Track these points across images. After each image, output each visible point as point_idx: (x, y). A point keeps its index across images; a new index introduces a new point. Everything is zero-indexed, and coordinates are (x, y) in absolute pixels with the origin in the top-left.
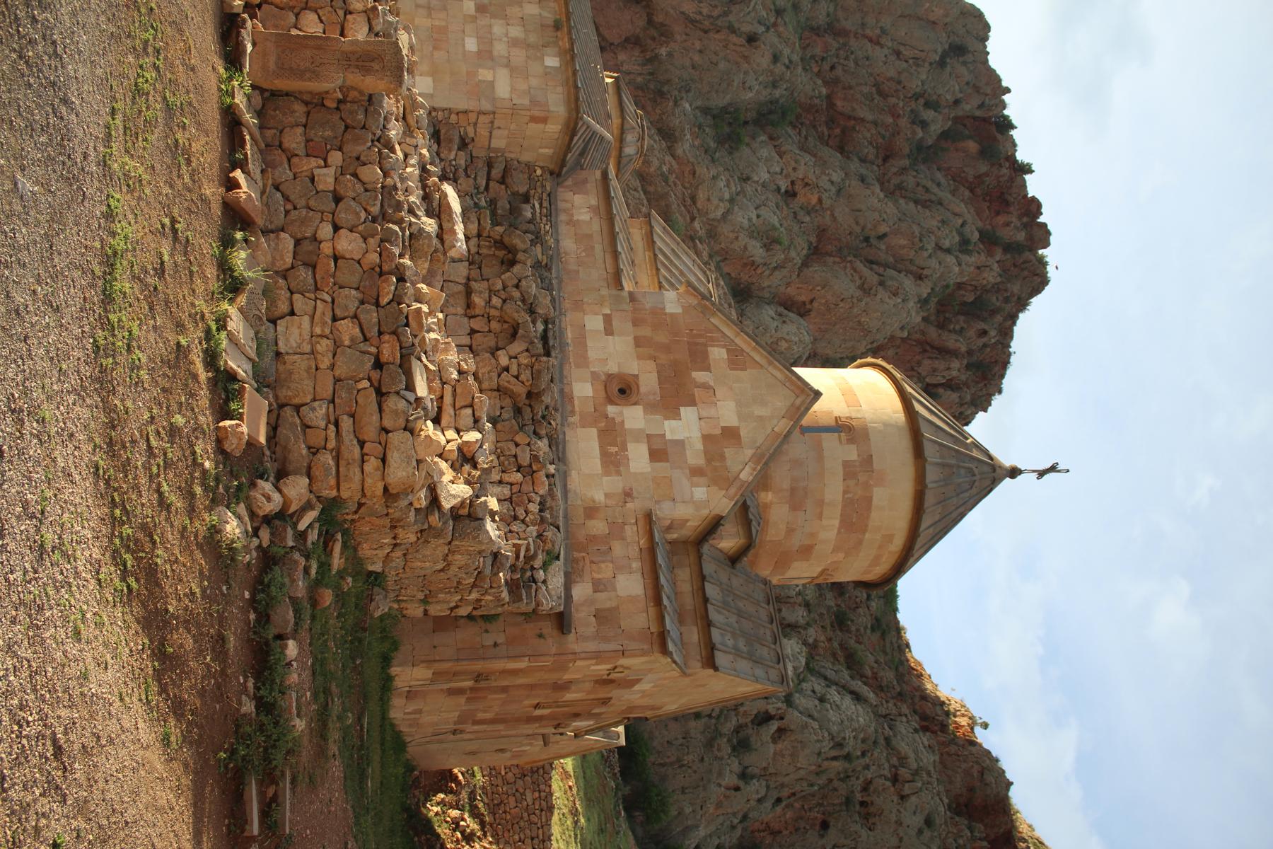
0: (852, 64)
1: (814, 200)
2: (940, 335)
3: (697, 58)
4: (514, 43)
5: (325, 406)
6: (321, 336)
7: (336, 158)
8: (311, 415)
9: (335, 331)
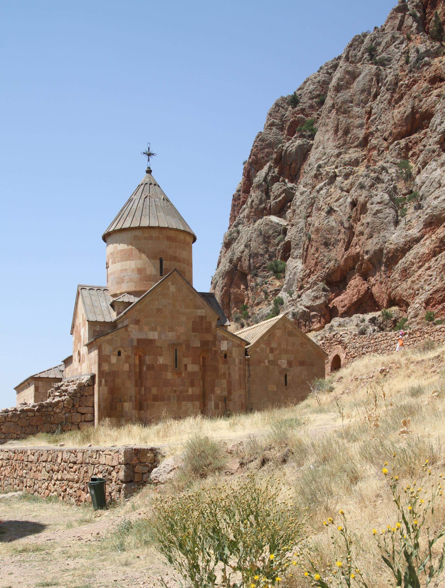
3: (366, 236)
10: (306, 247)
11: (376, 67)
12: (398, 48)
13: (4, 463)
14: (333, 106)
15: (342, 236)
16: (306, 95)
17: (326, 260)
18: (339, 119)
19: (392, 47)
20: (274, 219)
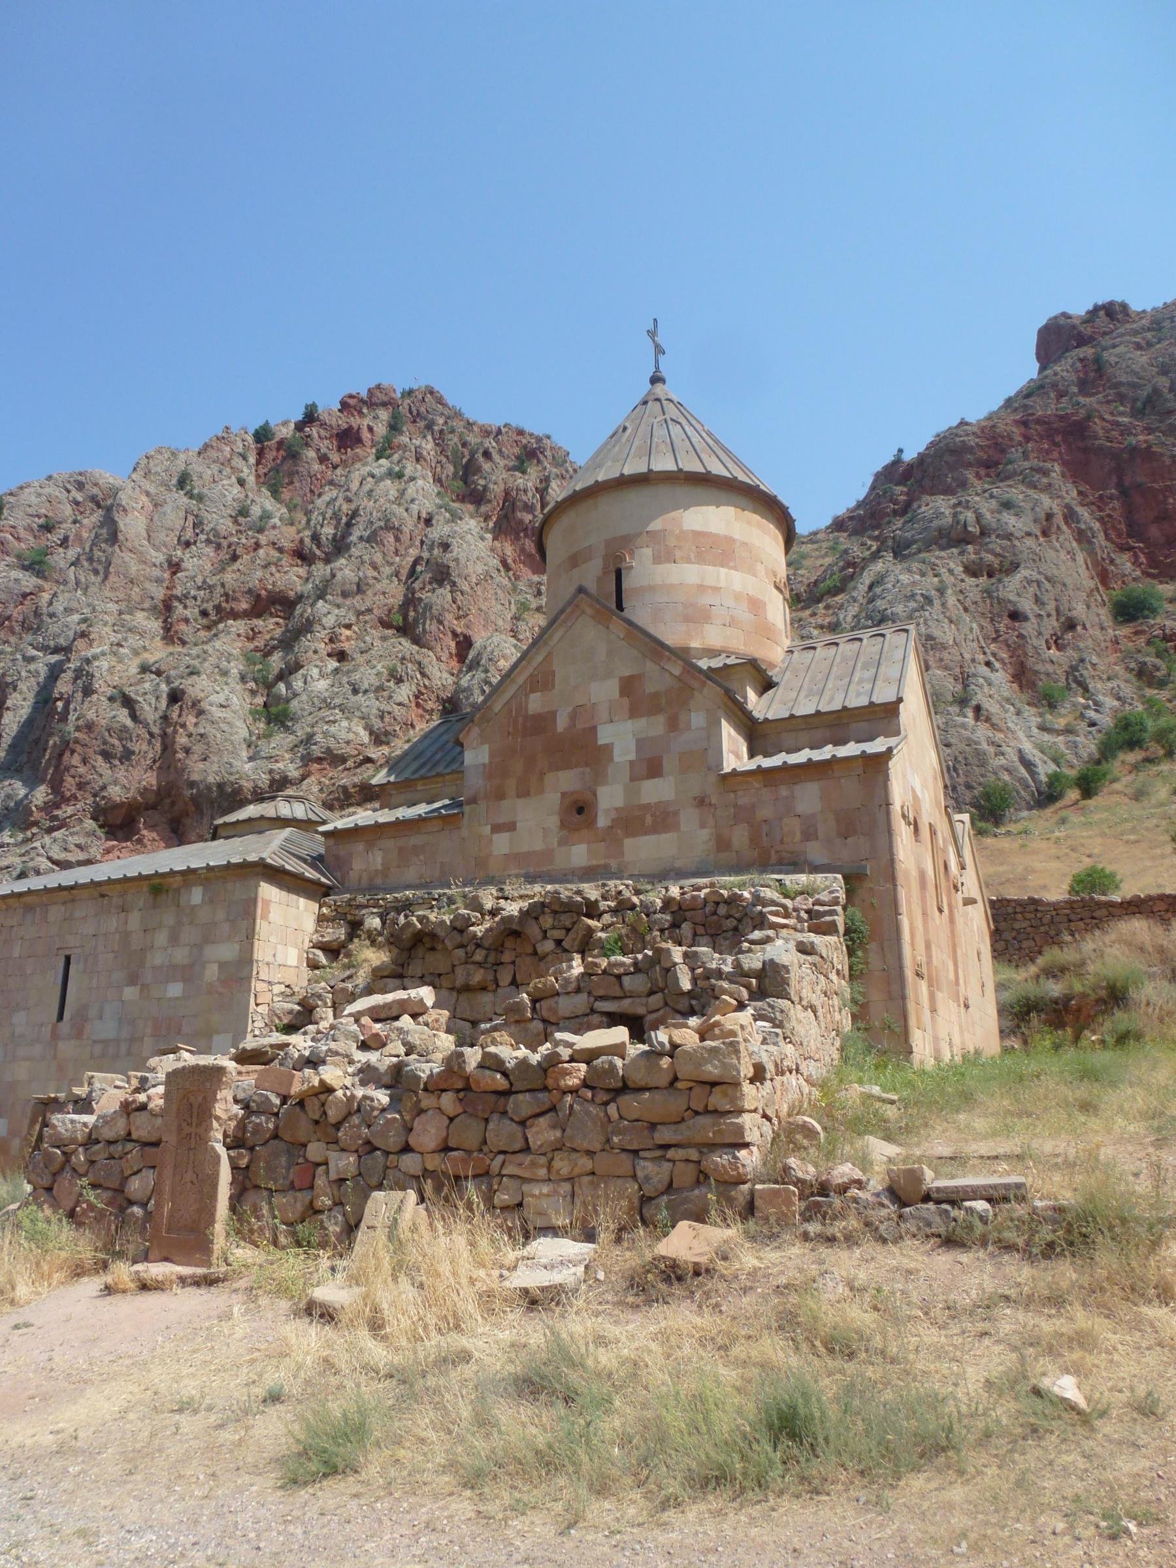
0: (202, 592)
1: (348, 633)
2: (490, 501)
4: (174, 939)
5: (642, 1163)
6: (549, 1168)
7: (315, 1151)
8: (655, 1180)
9: (543, 1150)
15: (145, 747)
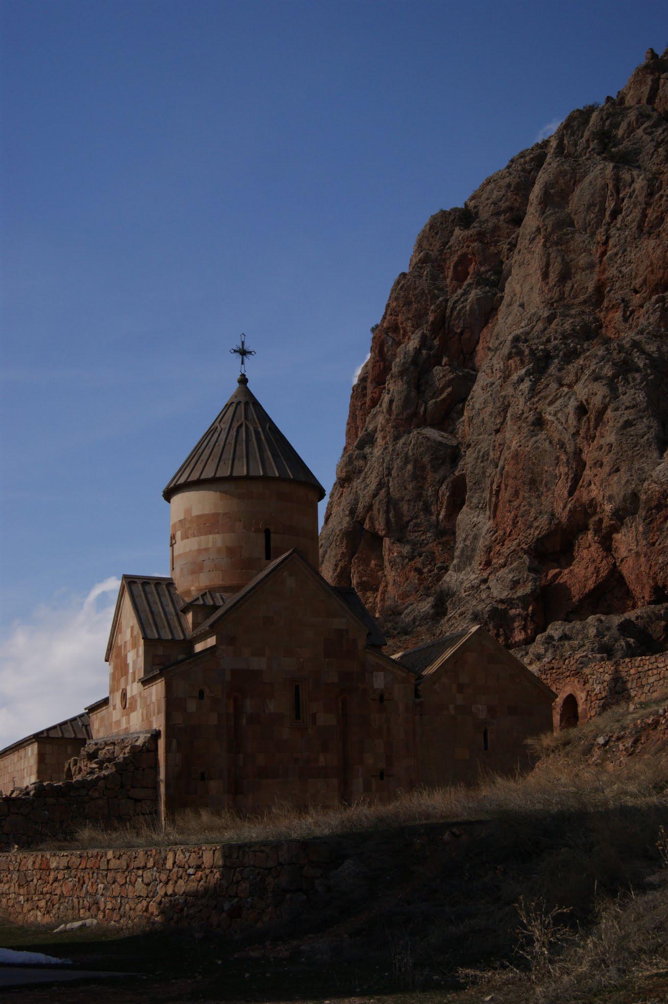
3: (607, 469)
10: (495, 487)
11: (611, 165)
12: (650, 134)
13: (59, 875)
14: (538, 230)
15: (563, 469)
16: (487, 208)
17: (533, 514)
18: (549, 255)
19: (640, 132)
20: (432, 433)
